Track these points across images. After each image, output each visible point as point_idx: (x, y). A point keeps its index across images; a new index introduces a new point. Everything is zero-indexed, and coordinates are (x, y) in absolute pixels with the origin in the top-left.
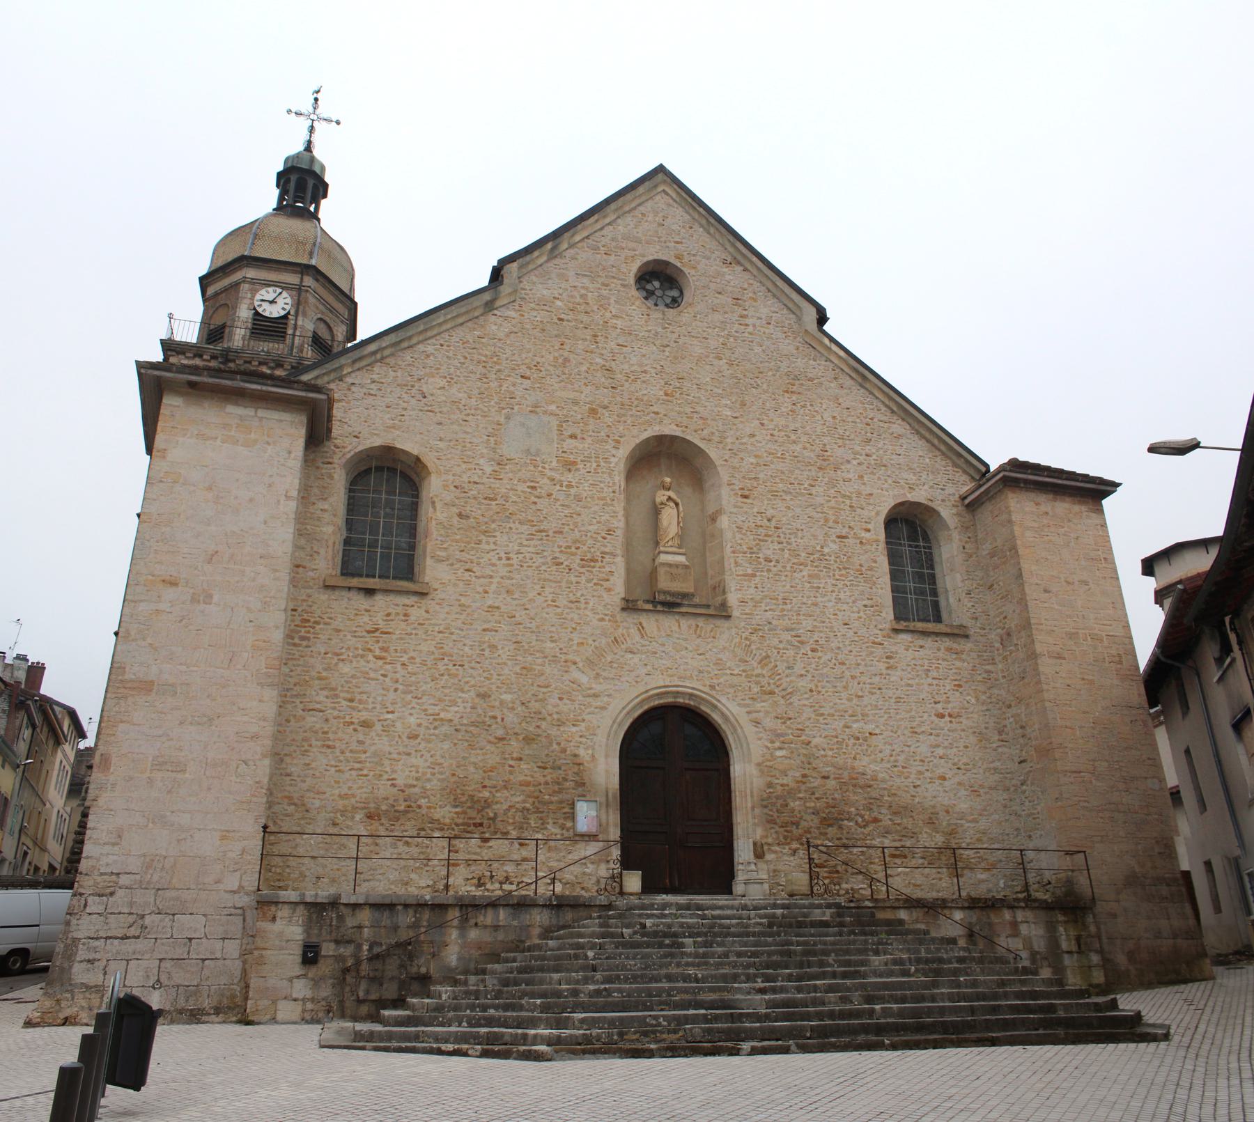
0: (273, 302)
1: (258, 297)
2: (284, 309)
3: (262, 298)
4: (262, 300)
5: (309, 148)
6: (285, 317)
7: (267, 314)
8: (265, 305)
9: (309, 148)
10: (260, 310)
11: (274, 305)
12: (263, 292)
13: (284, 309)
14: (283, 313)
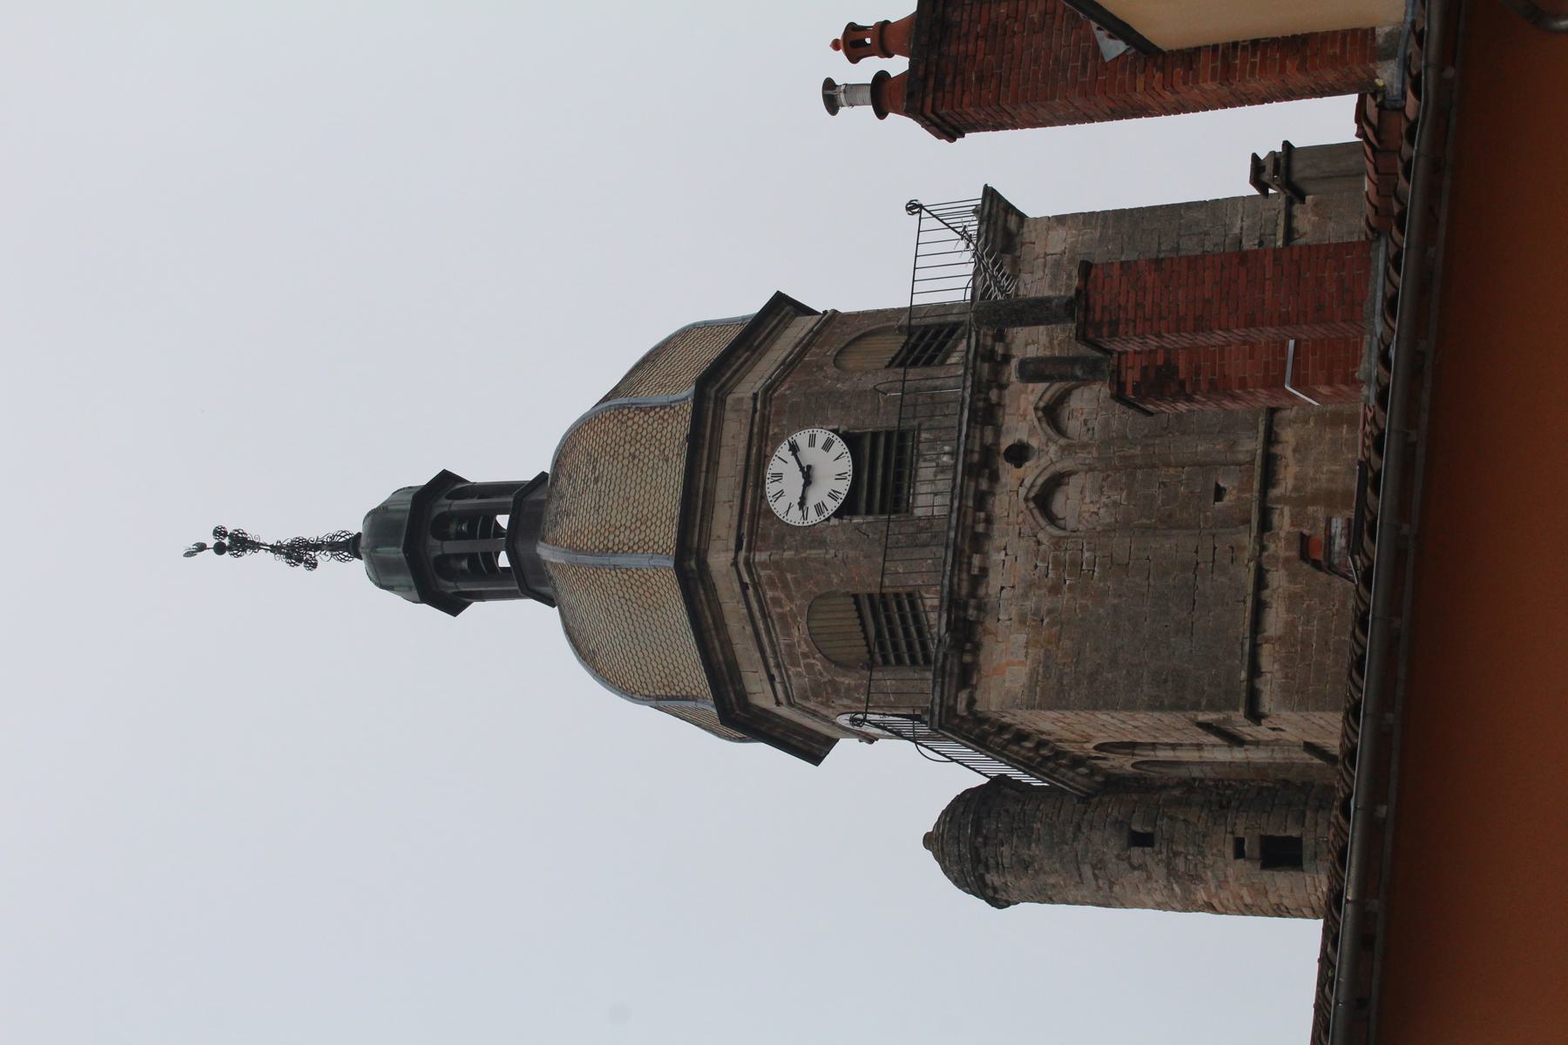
0: (808, 474)
1: (795, 518)
2: (827, 446)
3: (795, 510)
4: (802, 504)
5: (347, 547)
6: (852, 440)
7: (843, 487)
8: (816, 495)
9: (347, 547)
10: (832, 506)
11: (818, 473)
12: (779, 508)
13: (827, 446)
14: (839, 446)
